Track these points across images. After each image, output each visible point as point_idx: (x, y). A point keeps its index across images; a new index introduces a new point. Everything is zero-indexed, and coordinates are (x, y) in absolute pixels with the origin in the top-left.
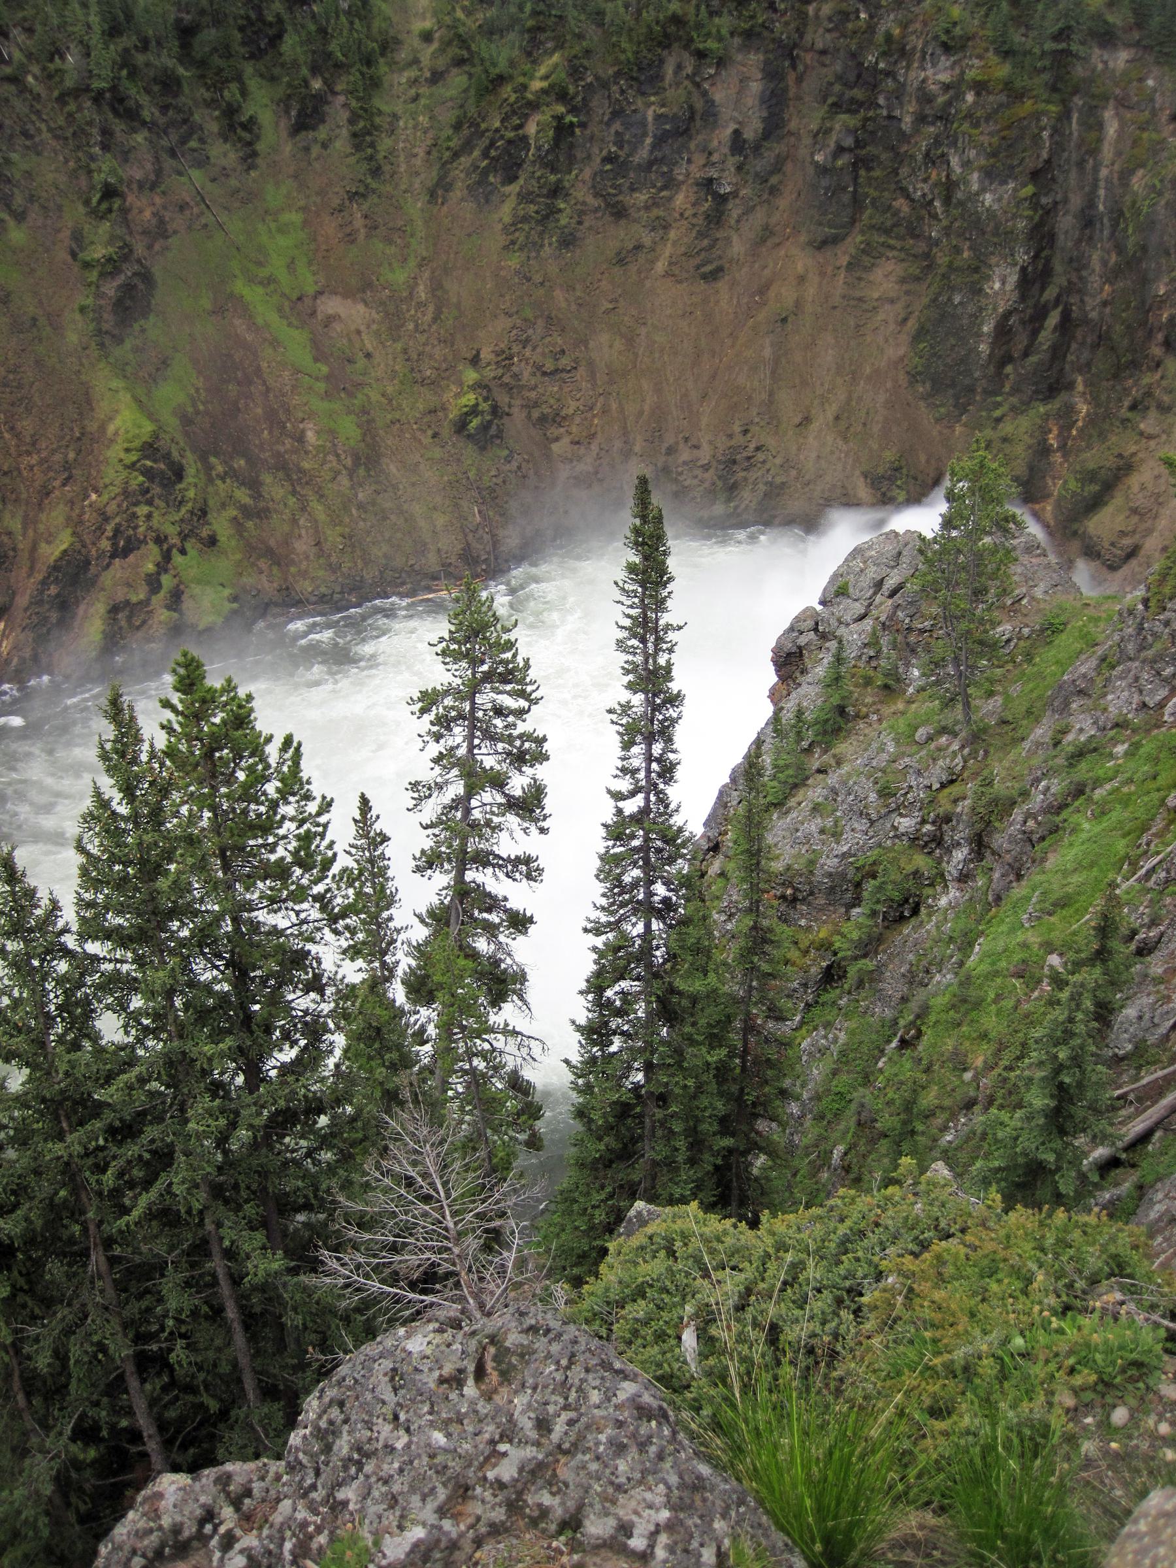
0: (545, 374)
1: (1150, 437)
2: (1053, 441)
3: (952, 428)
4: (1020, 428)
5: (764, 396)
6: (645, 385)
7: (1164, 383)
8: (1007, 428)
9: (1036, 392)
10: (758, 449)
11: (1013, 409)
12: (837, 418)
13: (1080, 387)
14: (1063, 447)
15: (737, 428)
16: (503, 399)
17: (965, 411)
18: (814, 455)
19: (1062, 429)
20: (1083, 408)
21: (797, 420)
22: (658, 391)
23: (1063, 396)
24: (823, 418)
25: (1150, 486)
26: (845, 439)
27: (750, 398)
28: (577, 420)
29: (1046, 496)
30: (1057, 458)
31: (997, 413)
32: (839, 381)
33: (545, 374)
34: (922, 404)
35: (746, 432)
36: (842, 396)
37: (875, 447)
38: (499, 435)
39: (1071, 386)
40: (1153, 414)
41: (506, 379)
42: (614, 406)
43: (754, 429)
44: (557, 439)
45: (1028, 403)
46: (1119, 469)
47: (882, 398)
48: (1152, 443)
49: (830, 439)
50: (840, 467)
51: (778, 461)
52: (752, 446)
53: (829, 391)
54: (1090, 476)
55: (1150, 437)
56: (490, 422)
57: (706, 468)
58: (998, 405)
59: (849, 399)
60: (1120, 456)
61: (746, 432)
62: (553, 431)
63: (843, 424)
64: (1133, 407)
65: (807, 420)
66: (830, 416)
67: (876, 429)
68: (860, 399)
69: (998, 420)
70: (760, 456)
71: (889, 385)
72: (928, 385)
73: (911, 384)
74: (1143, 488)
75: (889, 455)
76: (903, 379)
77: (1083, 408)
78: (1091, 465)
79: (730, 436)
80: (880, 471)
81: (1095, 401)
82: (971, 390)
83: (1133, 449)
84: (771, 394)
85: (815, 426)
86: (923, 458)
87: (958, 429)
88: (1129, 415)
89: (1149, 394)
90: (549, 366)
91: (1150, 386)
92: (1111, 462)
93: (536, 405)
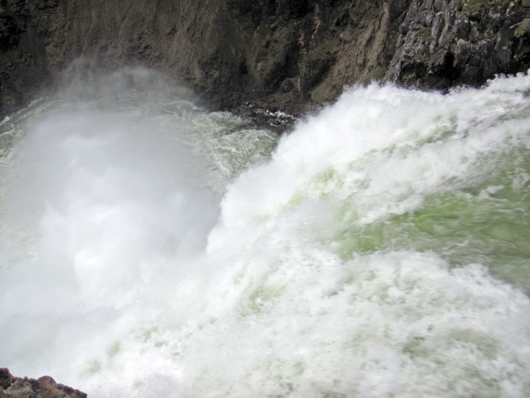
0: (40, 9)
1: (346, 42)
2: (301, 41)
3: (252, 34)
4: (282, 34)
5: (151, 18)
6: (94, 13)
7: (354, 9)
8: (277, 34)
9: (292, 13)
10: (146, 47)
11: (280, 23)
12: (188, 29)
13: (317, 10)
14: (307, 45)
15: (135, 37)
16: (20, 23)
17: (258, 24)
18: (175, 50)
19: (306, 35)
20: (318, 23)
21: (168, 31)
22: (99, 16)
23: (309, 15)
24: (181, 30)
25: (343, 72)
26: (192, 42)
27: (144, 19)
28: (57, 34)
29: (296, 73)
30: (304, 51)
31: (272, 26)
32: (192, 8)
33: (40, 9)
34: (236, 20)
35: (140, 38)
36: (192, 16)
37: (206, 46)
38: (16, 42)
39: (312, 10)
40: (349, 27)
41: (22, 12)
42: (75, 25)
43: (145, 37)
44: (48, 44)
45: (288, 21)
46: (328, 61)
47: (213, 17)
48: (347, 46)
49: (184, 41)
50: (187, 58)
51: (156, 54)
52: (143, 46)
53: (187, 14)
54: (312, 65)
55: (346, 42)
56: (8, 37)
57: (120, 57)
58: (273, 21)
59: (196, 18)
60: (328, 53)
61: (140, 38)
62: (46, 40)
63: (191, 33)
64: (338, 24)
65: (174, 30)
66: (186, 28)
67: (207, 35)
68: (201, 18)
69: (274, 29)
70: (148, 52)
71: (217, 10)
72: (238, 10)
73: (229, 9)
74: (339, 73)
75: (211, 51)
76: (225, 7)
77: (318, 23)
78: (314, 58)
79: (131, 41)
80: (205, 60)
81: (323, 19)
82: (259, 12)
83: (335, 49)
84: (155, 17)
85: (178, 34)
86: (233, 51)
87: (256, 34)
88: (335, 28)
89: (346, 16)
90: (42, 5)
91: (347, 11)
92: (324, 57)
93: (37, 26)
